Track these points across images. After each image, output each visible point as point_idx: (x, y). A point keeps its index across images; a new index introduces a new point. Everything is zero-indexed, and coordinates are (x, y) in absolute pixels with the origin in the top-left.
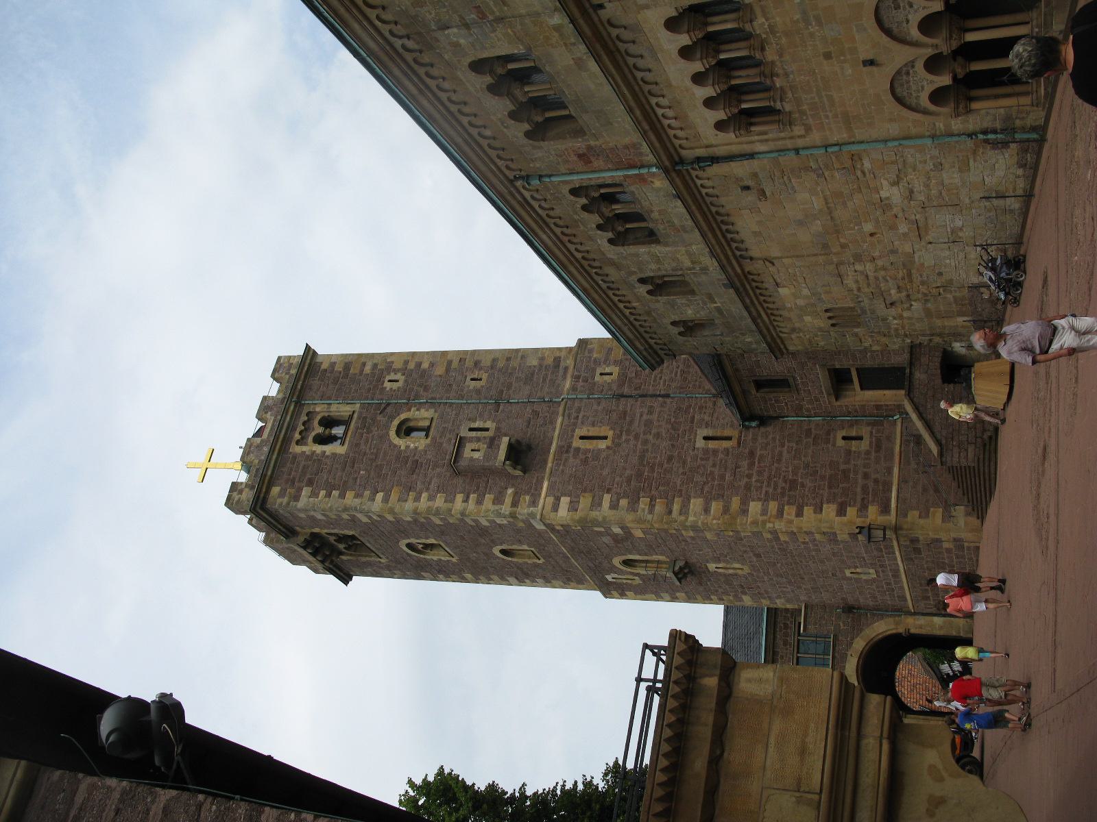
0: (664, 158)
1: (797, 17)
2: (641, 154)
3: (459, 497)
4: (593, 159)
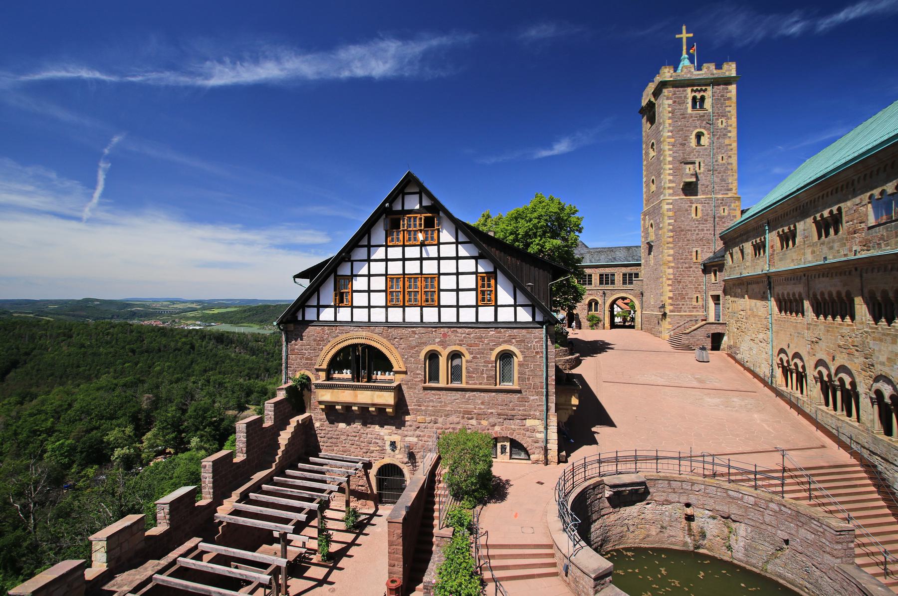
3: (671, 166)
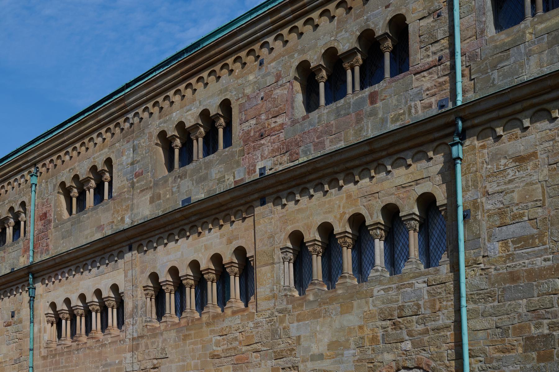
0: (37, 268)
1: (109, 361)
2: (42, 253)
4: (43, 221)
